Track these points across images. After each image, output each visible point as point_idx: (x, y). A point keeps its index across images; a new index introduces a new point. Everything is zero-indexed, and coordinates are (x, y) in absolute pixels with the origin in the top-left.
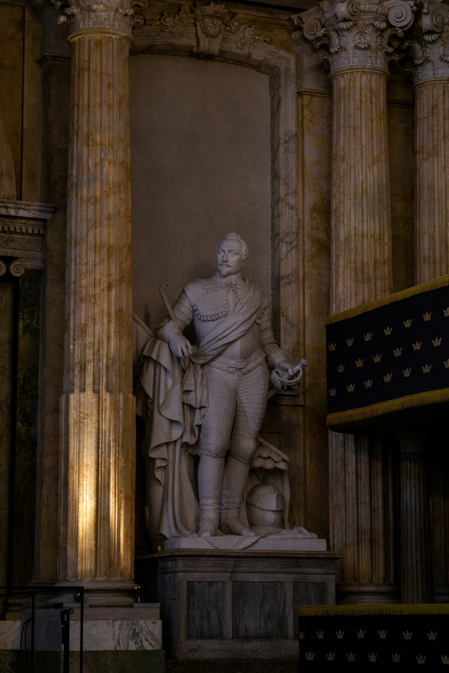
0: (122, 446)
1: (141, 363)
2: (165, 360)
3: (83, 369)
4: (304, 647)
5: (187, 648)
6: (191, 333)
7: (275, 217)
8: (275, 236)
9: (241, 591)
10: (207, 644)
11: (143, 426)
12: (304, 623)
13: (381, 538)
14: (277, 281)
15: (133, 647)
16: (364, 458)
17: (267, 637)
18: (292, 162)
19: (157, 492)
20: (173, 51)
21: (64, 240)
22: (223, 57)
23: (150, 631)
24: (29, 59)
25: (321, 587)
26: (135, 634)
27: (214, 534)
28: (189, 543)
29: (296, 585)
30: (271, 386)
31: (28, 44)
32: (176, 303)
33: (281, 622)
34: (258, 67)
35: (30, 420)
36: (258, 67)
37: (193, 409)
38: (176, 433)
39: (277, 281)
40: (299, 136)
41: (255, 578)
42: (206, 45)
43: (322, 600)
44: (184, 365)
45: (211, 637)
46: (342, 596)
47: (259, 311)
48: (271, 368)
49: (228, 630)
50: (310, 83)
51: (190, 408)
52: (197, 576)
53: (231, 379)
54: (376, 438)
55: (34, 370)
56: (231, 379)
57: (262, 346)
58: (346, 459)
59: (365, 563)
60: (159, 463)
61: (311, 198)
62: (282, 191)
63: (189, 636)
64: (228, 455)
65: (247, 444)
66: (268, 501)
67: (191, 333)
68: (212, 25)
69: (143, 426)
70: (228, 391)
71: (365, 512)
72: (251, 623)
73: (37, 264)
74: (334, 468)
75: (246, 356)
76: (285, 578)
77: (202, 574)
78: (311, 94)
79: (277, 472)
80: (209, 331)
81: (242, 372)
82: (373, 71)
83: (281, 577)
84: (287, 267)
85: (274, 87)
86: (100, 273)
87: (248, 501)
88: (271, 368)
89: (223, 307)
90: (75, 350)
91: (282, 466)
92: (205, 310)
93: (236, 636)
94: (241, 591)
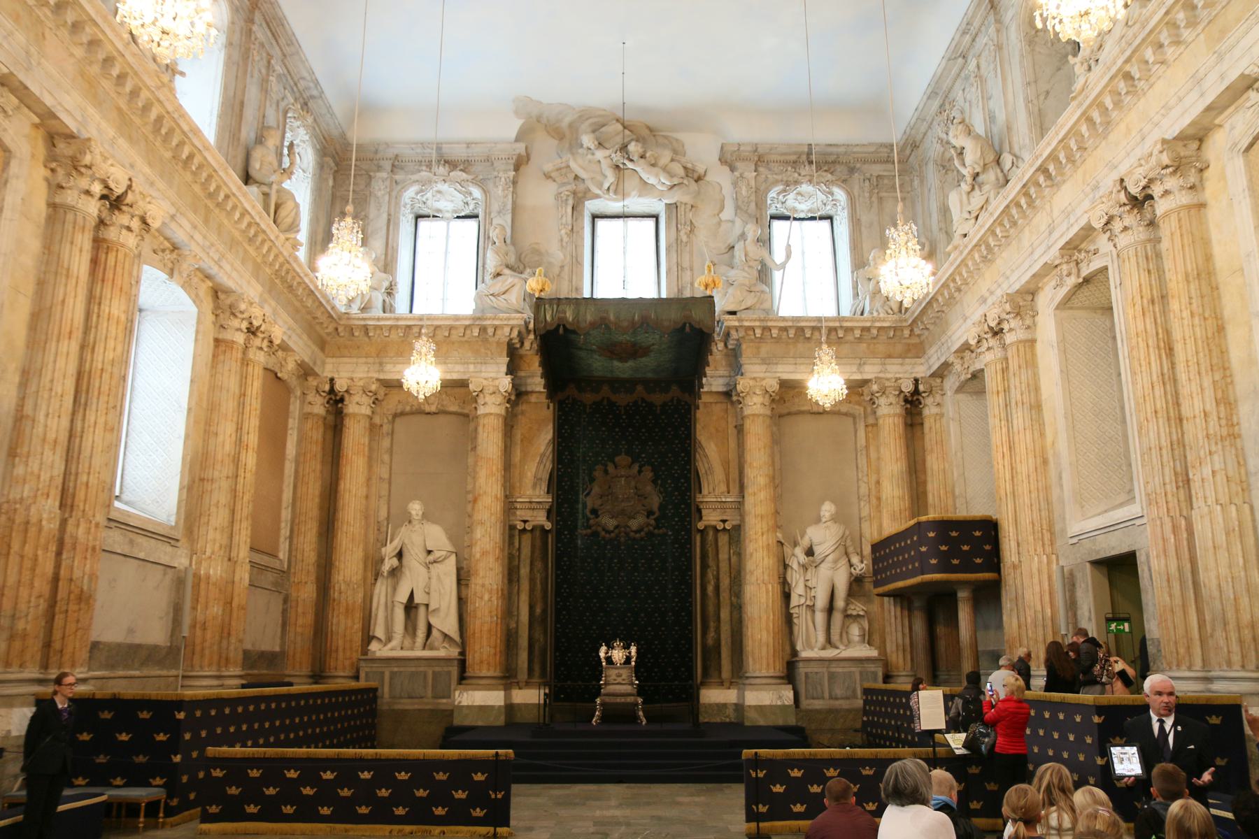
2: (795, 566)
4: (866, 702)
5: (805, 703)
6: (810, 552)
9: (832, 676)
10: (816, 702)
11: (787, 596)
12: (866, 691)
14: (860, 519)
15: (779, 703)
16: (899, 609)
17: (847, 698)
19: (796, 629)
23: (787, 695)
25: (875, 674)
26: (780, 697)
27: (823, 648)
29: (861, 673)
31: (730, 419)
33: (854, 691)
34: (846, 414)
38: (803, 600)
40: (867, 447)
41: (840, 670)
44: (805, 567)
46: (887, 678)
48: (851, 566)
49: (827, 695)
52: (809, 670)
53: (829, 573)
56: (829, 573)
57: (847, 554)
61: (874, 478)
65: (840, 603)
66: (855, 631)
71: (900, 635)
72: (838, 692)
75: (836, 561)
76: (855, 670)
81: (834, 569)
82: (895, 415)
83: (853, 669)
84: (865, 513)
85: (855, 423)
87: (844, 630)
88: (851, 566)
89: (823, 537)
91: (861, 613)
92: (815, 541)
93: (831, 698)
94: (832, 676)
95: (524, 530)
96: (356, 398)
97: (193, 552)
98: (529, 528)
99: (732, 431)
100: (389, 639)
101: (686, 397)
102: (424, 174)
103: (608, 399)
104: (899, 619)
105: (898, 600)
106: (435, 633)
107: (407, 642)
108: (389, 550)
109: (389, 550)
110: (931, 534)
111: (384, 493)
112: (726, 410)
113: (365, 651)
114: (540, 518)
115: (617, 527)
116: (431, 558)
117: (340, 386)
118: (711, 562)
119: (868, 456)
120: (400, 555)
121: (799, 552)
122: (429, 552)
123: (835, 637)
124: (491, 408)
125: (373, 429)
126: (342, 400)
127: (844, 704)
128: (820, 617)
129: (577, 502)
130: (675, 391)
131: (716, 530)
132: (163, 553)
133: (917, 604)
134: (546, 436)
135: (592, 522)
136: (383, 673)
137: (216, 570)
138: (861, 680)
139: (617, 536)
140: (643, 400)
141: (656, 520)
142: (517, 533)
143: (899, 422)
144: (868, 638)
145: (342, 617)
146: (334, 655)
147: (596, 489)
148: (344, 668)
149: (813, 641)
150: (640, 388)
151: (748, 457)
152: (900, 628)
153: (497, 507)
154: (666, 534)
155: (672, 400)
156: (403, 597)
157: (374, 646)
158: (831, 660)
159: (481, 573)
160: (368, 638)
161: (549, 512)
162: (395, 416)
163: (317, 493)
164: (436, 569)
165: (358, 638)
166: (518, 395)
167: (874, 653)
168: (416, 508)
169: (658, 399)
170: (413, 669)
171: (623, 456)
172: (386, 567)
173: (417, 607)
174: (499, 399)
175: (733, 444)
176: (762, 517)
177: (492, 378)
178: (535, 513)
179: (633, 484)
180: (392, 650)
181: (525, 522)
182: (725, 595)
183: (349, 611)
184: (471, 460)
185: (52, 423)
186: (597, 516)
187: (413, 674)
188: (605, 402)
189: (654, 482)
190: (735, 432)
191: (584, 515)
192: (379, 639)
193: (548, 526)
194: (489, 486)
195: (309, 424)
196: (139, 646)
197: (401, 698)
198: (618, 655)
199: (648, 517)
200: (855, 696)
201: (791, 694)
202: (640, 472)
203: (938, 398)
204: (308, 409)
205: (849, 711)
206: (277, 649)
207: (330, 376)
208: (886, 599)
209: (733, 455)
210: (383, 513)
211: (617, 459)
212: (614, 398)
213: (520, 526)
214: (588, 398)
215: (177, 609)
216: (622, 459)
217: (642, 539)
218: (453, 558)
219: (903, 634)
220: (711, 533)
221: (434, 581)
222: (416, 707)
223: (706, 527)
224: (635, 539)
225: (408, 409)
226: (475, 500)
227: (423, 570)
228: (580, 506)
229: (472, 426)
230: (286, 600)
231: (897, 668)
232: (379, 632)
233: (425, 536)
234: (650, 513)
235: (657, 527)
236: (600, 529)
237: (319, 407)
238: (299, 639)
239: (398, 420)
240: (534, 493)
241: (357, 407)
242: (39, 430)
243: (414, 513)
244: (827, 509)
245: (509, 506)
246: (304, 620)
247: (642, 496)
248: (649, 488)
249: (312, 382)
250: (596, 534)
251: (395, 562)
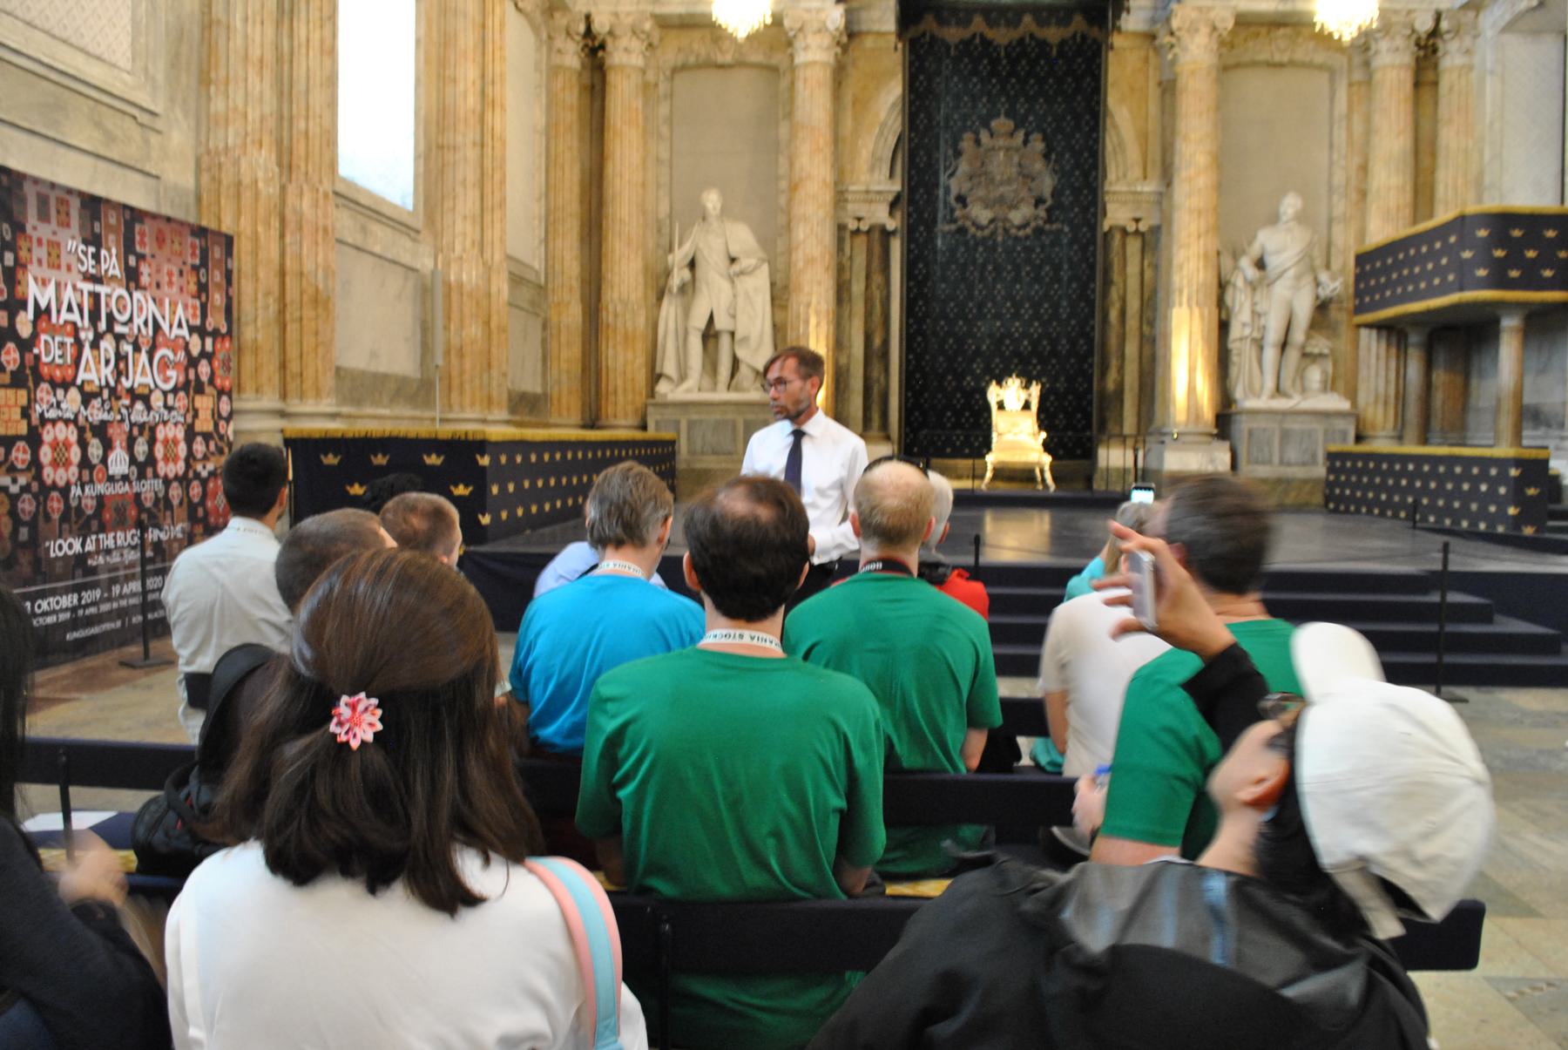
0: (1207, 341)
1: (1222, 286)
2: (1240, 283)
3: (1181, 292)
4: (1331, 470)
6: (1260, 264)
7: (1331, 175)
8: (1331, 190)
9: (1285, 435)
11: (1224, 327)
12: (1332, 457)
13: (1392, 400)
14: (1330, 221)
16: (1383, 344)
17: (1304, 464)
18: (1344, 135)
19: (1233, 371)
20: (1254, 64)
21: (1171, 206)
22: (1292, 63)
24: (1152, 84)
25: (1344, 434)
27: (1272, 397)
28: (1251, 403)
29: (1326, 432)
30: (1317, 297)
31: (1151, 73)
32: (1250, 243)
33: (1314, 456)
34: (1320, 67)
35: (1152, 324)
36: (1320, 67)
37: (1259, 315)
38: (1247, 331)
39: (1330, 221)
40: (1349, 116)
41: (1297, 426)
42: (1277, 58)
43: (1344, 440)
44: (1253, 286)
45: (1263, 463)
46: (1359, 438)
47: (1310, 245)
48: (1318, 284)
49: (1276, 459)
50: (1358, 75)
51: (1256, 314)
52: (1255, 425)
54: (1393, 331)
55: (1154, 292)
56: (1287, 293)
58: (1371, 343)
59: (1380, 417)
60: (1235, 352)
61: (1356, 160)
62: (1335, 156)
63: (1249, 462)
64: (1284, 346)
65: (1298, 336)
66: (1315, 375)
67: (1260, 264)
68: (1282, 44)
69: (1224, 327)
70: (1287, 299)
72: (1292, 454)
73: (1154, 221)
74: (1362, 353)
75: (1298, 278)
76: (1318, 427)
77: (1258, 424)
78: (1360, 83)
79: (1321, 355)
80: (1272, 262)
81: (1296, 288)
85: (1332, 80)
86: (1193, 227)
87: (1301, 373)
89: (1282, 244)
90: (1176, 279)
91: (1326, 351)
94: (1285, 435)
95: (857, 232)
96: (624, 42)
97: (437, 250)
98: (864, 227)
99: (1153, 92)
100: (683, 377)
101: (1095, 32)
103: (982, 35)
104: (1382, 362)
105: (1384, 333)
106: (743, 369)
107: (706, 382)
108: (679, 257)
109: (679, 257)
110: (1482, 233)
111: (664, 179)
112: (1146, 60)
113: (652, 393)
114: (879, 214)
115: (992, 221)
116: (736, 267)
117: (601, 25)
118: (1116, 277)
119: (1349, 129)
120: (692, 265)
121: (1246, 263)
122: (733, 260)
123: (1286, 384)
124: (815, 54)
125: (647, 88)
126: (602, 47)
127: (1299, 472)
128: (1270, 354)
129: (937, 185)
130: (1078, 23)
131: (1124, 232)
132: (403, 249)
133: (1414, 338)
134: (892, 92)
135: (958, 213)
136: (678, 423)
137: (470, 275)
138: (1326, 441)
139: (994, 233)
140: (1032, 36)
141: (1048, 211)
142: (847, 235)
143: (1407, 77)
144: (1329, 385)
145: (620, 349)
146: (612, 398)
147: (963, 167)
148: (626, 415)
149: (1257, 386)
150: (1027, 19)
151: (1182, 126)
152: (1383, 373)
153: (827, 196)
154: (1060, 231)
155: (1074, 36)
156: (699, 322)
157: (663, 387)
158: (1284, 414)
159: (806, 289)
160: (655, 377)
161: (893, 206)
162: (675, 70)
163: (576, 178)
164: (747, 283)
165: (641, 377)
166: (851, 34)
167: (1344, 405)
168: (712, 200)
169: (1053, 34)
170: (718, 417)
171: (1002, 119)
172: (675, 282)
173: (717, 335)
174: (826, 41)
175: (1153, 108)
176: (1200, 213)
178: (873, 207)
179: (1016, 159)
180: (688, 391)
181: (859, 219)
182: (1132, 323)
183: (628, 339)
184: (783, 131)
185: (255, 33)
186: (965, 205)
187: (718, 425)
188: (977, 41)
189: (1046, 156)
190: (1158, 92)
191: (945, 203)
192: (669, 378)
193: (891, 225)
194: (814, 167)
195: (559, 84)
196: (385, 377)
197: (703, 453)
199: (1036, 206)
200: (1314, 461)
201: (1227, 457)
202: (1026, 142)
203: (1467, 42)
204: (557, 60)
205: (1305, 482)
206: (539, 390)
207: (585, 10)
208: (1364, 332)
209: (1153, 126)
210: (664, 209)
211: (994, 124)
212: (990, 34)
213: (852, 225)
214: (953, 34)
215: (425, 328)
216: (1001, 123)
217: (1027, 237)
218: (765, 267)
219: (1387, 382)
220: (1117, 237)
221: (741, 299)
222: (724, 465)
223: (1111, 229)
224: (1017, 239)
225: (692, 60)
226: (794, 188)
227: (725, 285)
228: (941, 192)
229: (784, 83)
230: (545, 327)
231: (1374, 427)
232: (669, 367)
233: (724, 238)
234: (1039, 201)
235: (1049, 220)
236: (968, 224)
237: (572, 58)
238: (564, 377)
239: (678, 78)
241: (625, 56)
242: (237, 42)
243: (709, 206)
244: (1290, 205)
245: (840, 198)
246: (569, 353)
247: (1027, 177)
248: (1039, 165)
249: (561, 20)
250: (962, 231)
251: (687, 274)
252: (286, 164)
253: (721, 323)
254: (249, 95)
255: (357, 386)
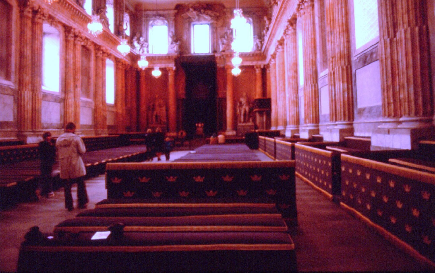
87: (249, 120)
102: (154, 18)
114: (183, 96)
134: (184, 79)
156: (155, 114)
172: (151, 108)
177: (172, 66)
198: (200, 125)
232: (150, 121)
237: (134, 74)
240: (182, 91)
252: (103, 105)
253: (158, 114)
254: (99, 98)
255: (109, 127)
